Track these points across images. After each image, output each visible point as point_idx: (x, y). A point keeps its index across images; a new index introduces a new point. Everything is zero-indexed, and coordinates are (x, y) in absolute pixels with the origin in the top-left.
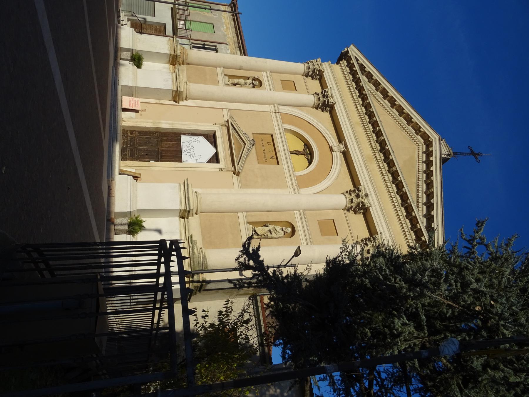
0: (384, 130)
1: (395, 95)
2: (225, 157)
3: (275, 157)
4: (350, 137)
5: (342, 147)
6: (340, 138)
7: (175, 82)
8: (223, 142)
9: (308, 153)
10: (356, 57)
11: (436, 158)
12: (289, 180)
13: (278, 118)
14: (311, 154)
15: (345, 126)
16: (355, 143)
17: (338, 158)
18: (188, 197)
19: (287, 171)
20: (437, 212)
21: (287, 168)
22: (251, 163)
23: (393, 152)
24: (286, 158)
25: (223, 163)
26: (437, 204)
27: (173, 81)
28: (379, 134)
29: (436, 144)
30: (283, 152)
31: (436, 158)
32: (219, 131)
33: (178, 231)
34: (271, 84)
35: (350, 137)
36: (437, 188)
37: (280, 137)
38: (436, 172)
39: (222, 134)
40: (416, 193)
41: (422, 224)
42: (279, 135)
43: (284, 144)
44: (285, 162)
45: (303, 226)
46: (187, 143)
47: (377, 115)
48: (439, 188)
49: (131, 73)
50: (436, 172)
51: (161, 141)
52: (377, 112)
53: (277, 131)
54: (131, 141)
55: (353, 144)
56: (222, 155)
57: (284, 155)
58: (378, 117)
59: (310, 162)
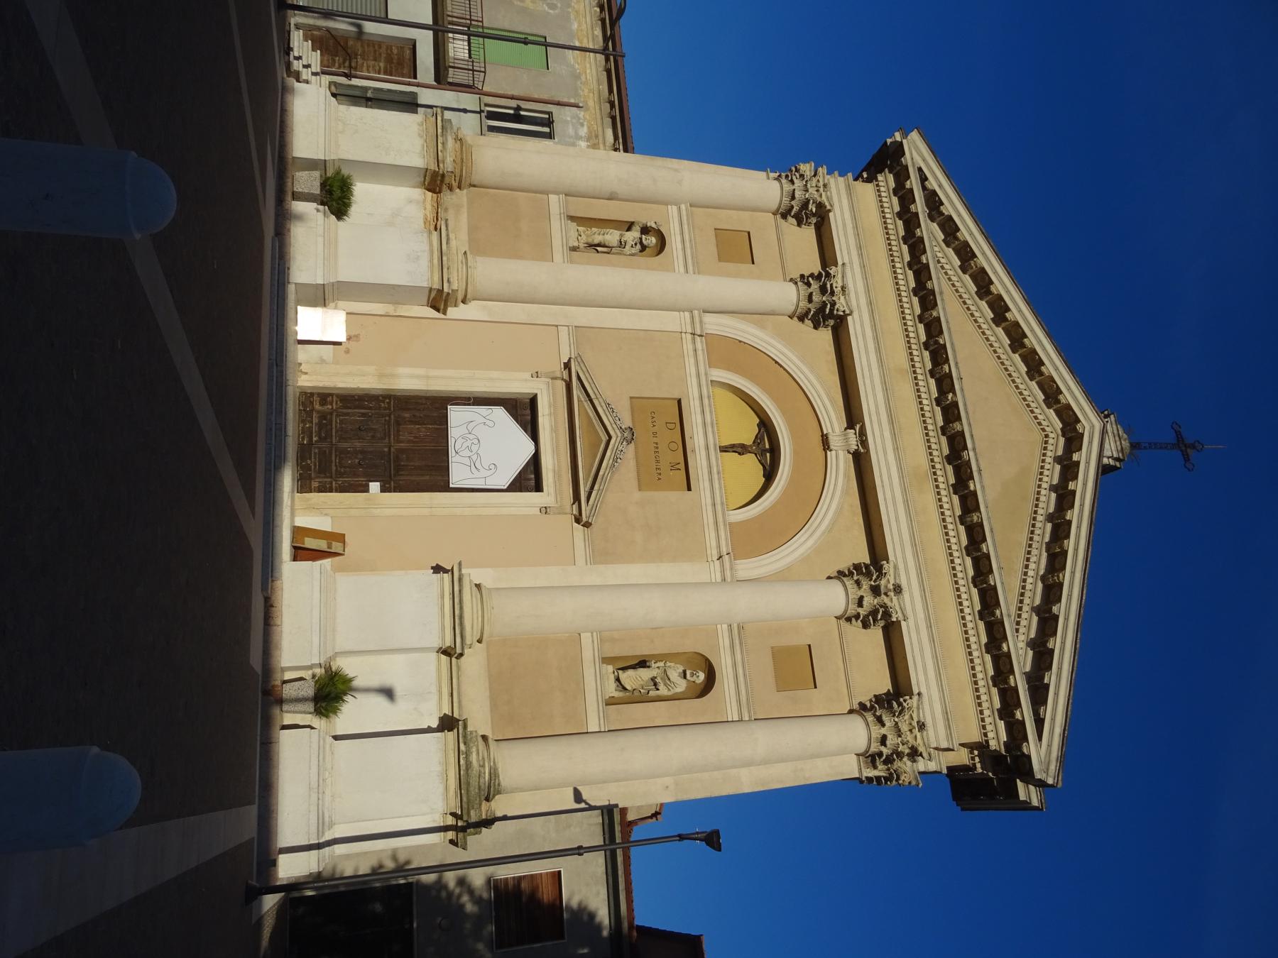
0: (965, 405)
1: (1008, 292)
2: (557, 474)
3: (682, 466)
4: (878, 414)
5: (853, 442)
6: (853, 416)
7: (436, 261)
8: (554, 430)
9: (766, 448)
10: (920, 169)
11: (1085, 484)
12: (713, 535)
13: (700, 352)
14: (775, 450)
15: (868, 382)
16: (887, 434)
17: (841, 464)
18: (461, 617)
19: (710, 508)
20: (1063, 643)
21: (709, 501)
22: (621, 490)
23: (980, 471)
24: (710, 472)
25: (552, 490)
26: (1066, 619)
27: (431, 261)
28: (951, 413)
29: (1090, 442)
30: (703, 453)
31: (1085, 484)
32: (545, 392)
33: (434, 689)
34: (687, 244)
35: (878, 414)
36: (1073, 573)
37: (698, 410)
38: (1079, 527)
39: (553, 405)
40: (1019, 575)
42: (697, 403)
43: (709, 429)
44: (707, 484)
45: (734, 665)
46: (463, 430)
47: (955, 357)
48: (1078, 575)
49: (320, 240)
50: (1079, 527)
51: (398, 423)
52: (954, 351)
53: (694, 392)
54: (320, 425)
55: (882, 435)
56: (550, 467)
57: (705, 463)
58: (956, 364)
59: (770, 475)
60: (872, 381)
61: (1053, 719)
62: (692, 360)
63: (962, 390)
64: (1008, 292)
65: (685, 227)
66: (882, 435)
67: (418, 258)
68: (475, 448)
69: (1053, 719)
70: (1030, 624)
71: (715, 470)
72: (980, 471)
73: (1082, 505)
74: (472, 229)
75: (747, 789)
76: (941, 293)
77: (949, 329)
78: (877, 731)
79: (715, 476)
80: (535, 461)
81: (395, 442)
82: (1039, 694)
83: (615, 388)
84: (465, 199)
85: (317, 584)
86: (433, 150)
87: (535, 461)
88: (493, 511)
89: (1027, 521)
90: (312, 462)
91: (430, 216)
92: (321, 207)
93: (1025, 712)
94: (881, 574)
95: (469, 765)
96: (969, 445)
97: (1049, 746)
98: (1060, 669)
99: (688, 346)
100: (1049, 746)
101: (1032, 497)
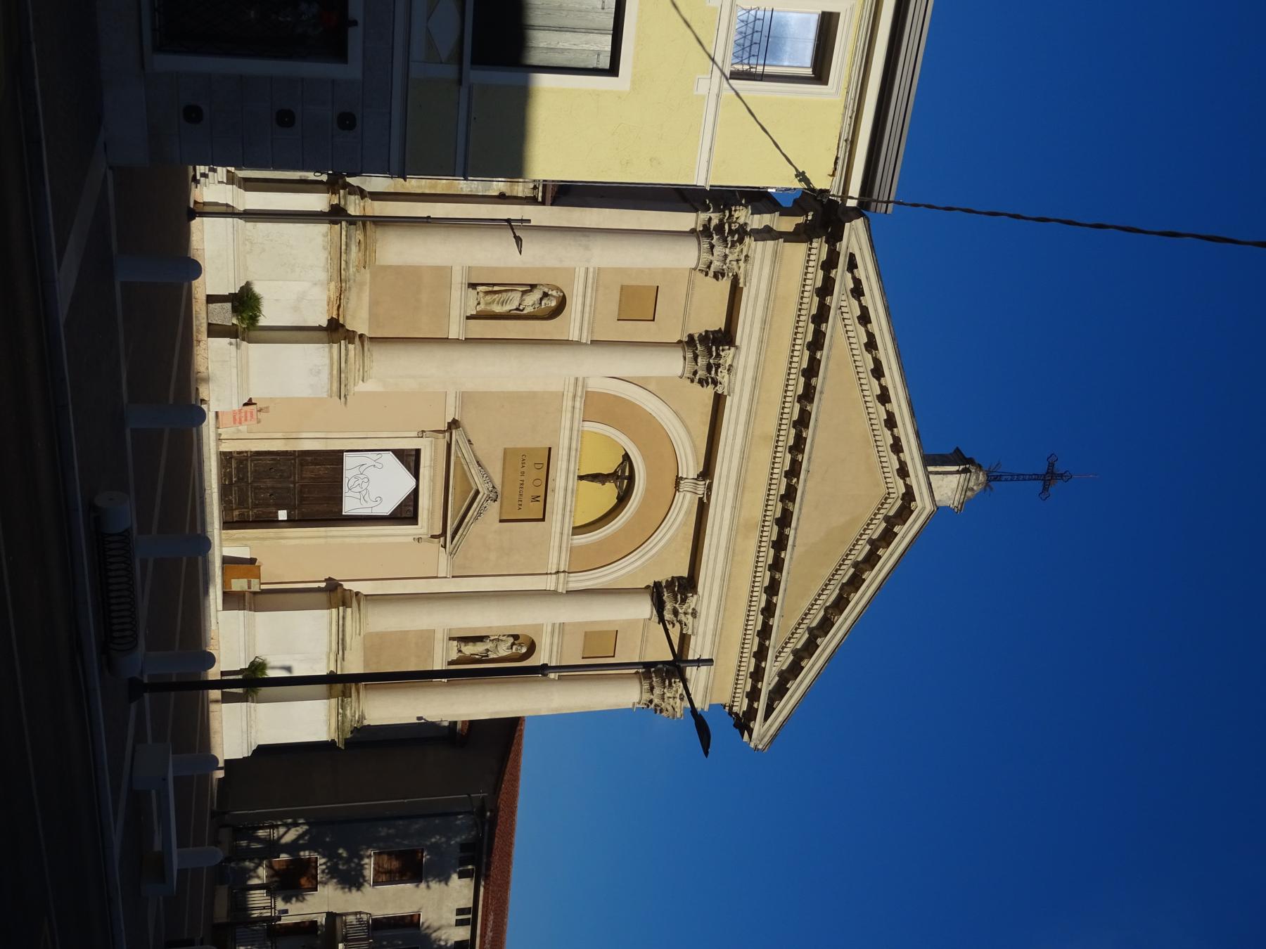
0: (803, 493)
1: (895, 387)
2: (431, 513)
3: (542, 499)
4: (728, 477)
5: (701, 490)
6: (707, 473)
7: (335, 372)
8: (433, 480)
9: (623, 477)
10: (852, 256)
11: (891, 555)
12: (556, 554)
13: (577, 411)
14: (631, 478)
15: (728, 449)
16: (730, 494)
17: (686, 503)
18: (343, 631)
19: (558, 535)
20: (813, 665)
21: (558, 530)
23: (794, 546)
24: (564, 509)
25: (425, 524)
26: (824, 650)
27: (331, 374)
28: (789, 495)
29: (915, 521)
30: (562, 493)
31: (891, 555)
32: (428, 450)
33: (325, 657)
34: (587, 309)
35: (728, 477)
36: (846, 619)
37: (565, 458)
38: (868, 587)
39: (434, 460)
40: (811, 600)
41: (766, 687)
42: (566, 452)
44: (560, 517)
45: (552, 644)
46: (356, 472)
47: (811, 453)
48: (849, 622)
49: (234, 371)
50: (868, 587)
51: (301, 465)
52: (812, 446)
53: (564, 442)
54: (238, 469)
55: (725, 496)
56: (426, 506)
57: (561, 500)
58: (809, 459)
59: (623, 499)
60: (732, 449)
61: (781, 712)
62: (569, 415)
63: (805, 481)
64: (895, 387)
65: (589, 290)
66: (725, 496)
67: (319, 372)
68: (364, 486)
69: (781, 712)
70: (786, 660)
71: (568, 508)
72: (794, 546)
73: (880, 571)
74: (374, 303)
75: (543, 713)
76: (821, 393)
77: (815, 427)
78: (647, 696)
79: (568, 514)
80: (415, 492)
81: (302, 487)
82: (779, 691)
83: (489, 443)
84: (368, 276)
85: (242, 624)
86: (336, 267)
87: (415, 492)
88: (375, 540)
89: (838, 559)
90: (234, 498)
91: (334, 295)
92: (233, 341)
93: (761, 706)
94: (684, 601)
95: (344, 715)
96: (793, 525)
97: (770, 726)
98: (802, 682)
99: (568, 403)
100: (770, 726)
101: (852, 541)
